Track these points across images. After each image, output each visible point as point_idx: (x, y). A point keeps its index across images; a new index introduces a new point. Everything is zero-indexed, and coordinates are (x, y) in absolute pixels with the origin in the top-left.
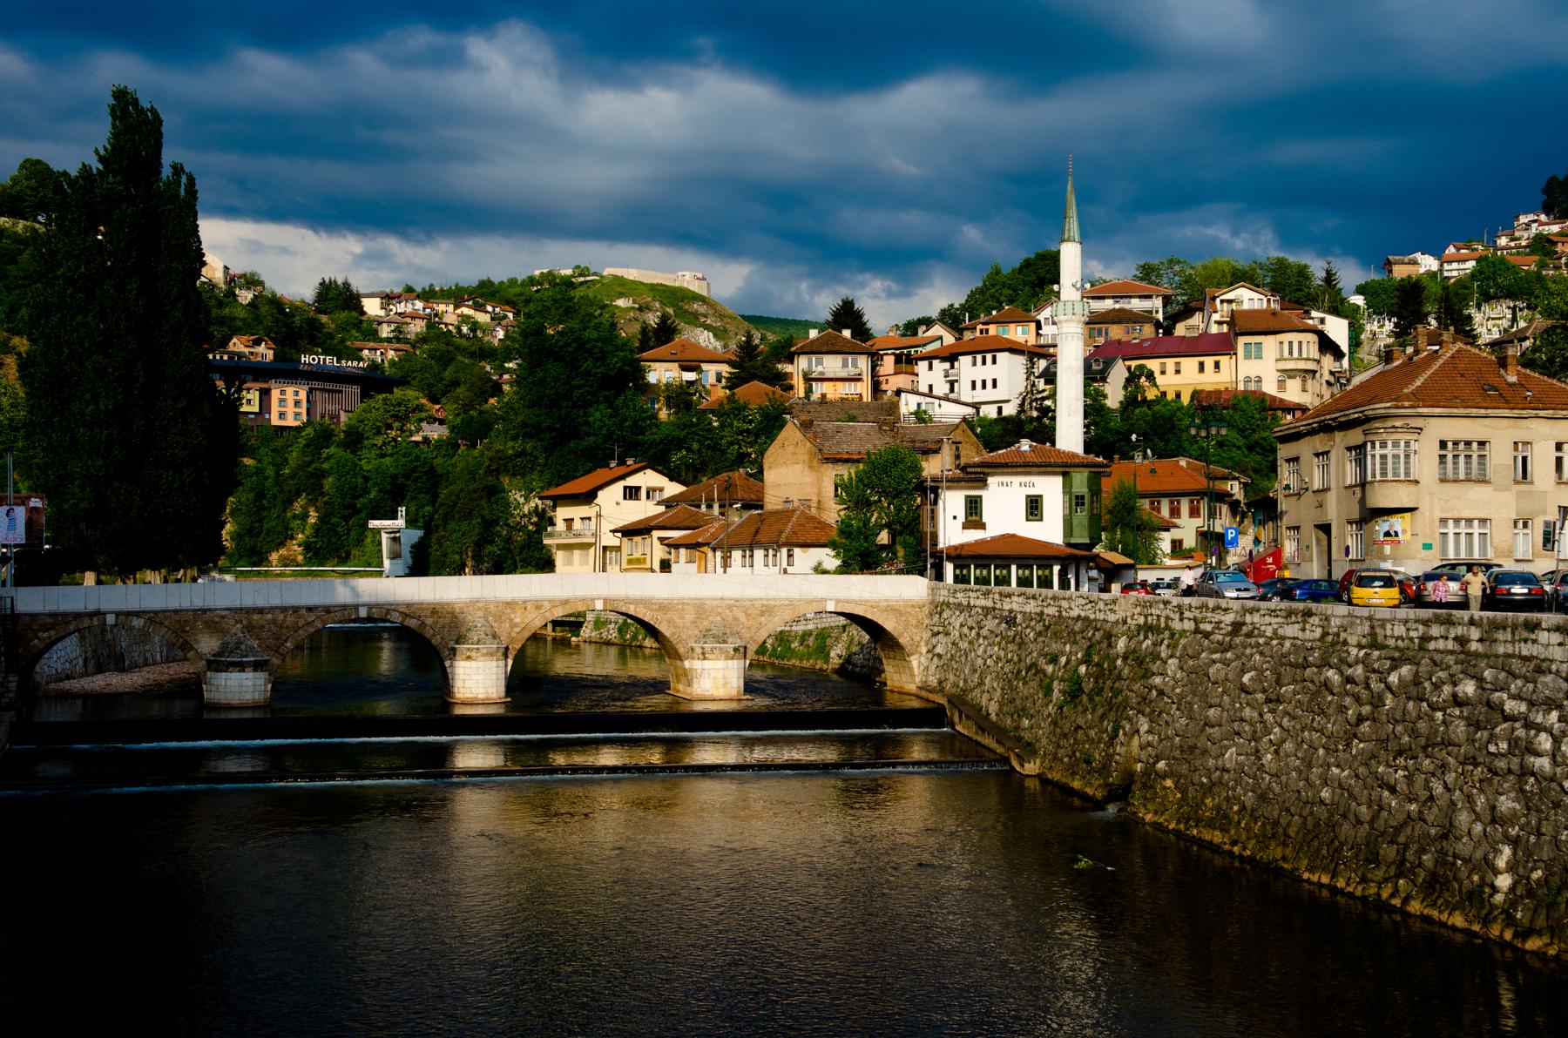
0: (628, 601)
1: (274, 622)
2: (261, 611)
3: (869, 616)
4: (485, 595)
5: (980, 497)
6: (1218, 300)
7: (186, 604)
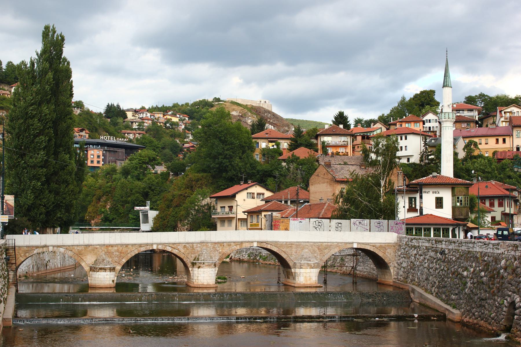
0: (267, 243)
1: (118, 251)
2: (112, 246)
3: (372, 250)
4: (206, 240)
6: (503, 112)
7: (81, 243)
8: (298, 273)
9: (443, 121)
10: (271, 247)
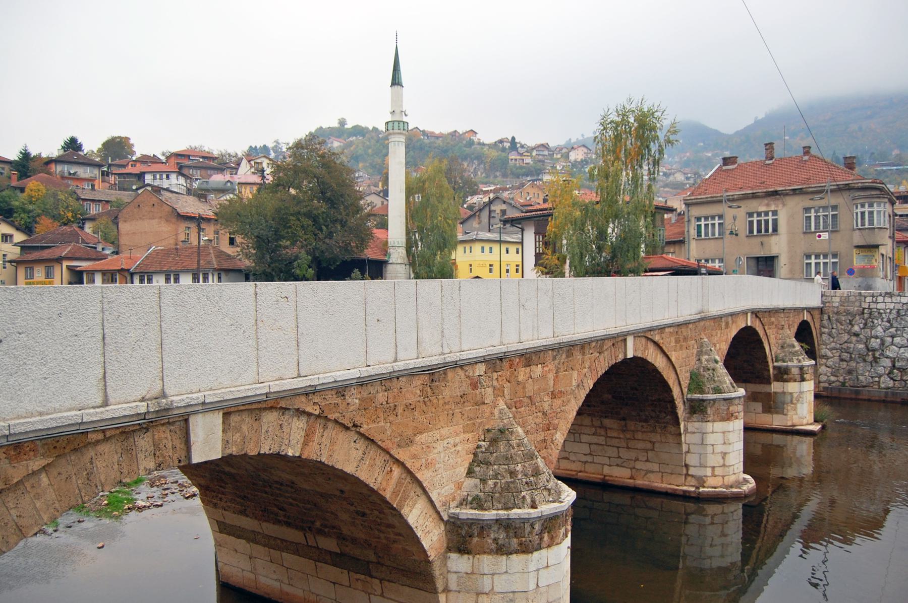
5: (777, 219)
8: (795, 395)
9: (394, 134)
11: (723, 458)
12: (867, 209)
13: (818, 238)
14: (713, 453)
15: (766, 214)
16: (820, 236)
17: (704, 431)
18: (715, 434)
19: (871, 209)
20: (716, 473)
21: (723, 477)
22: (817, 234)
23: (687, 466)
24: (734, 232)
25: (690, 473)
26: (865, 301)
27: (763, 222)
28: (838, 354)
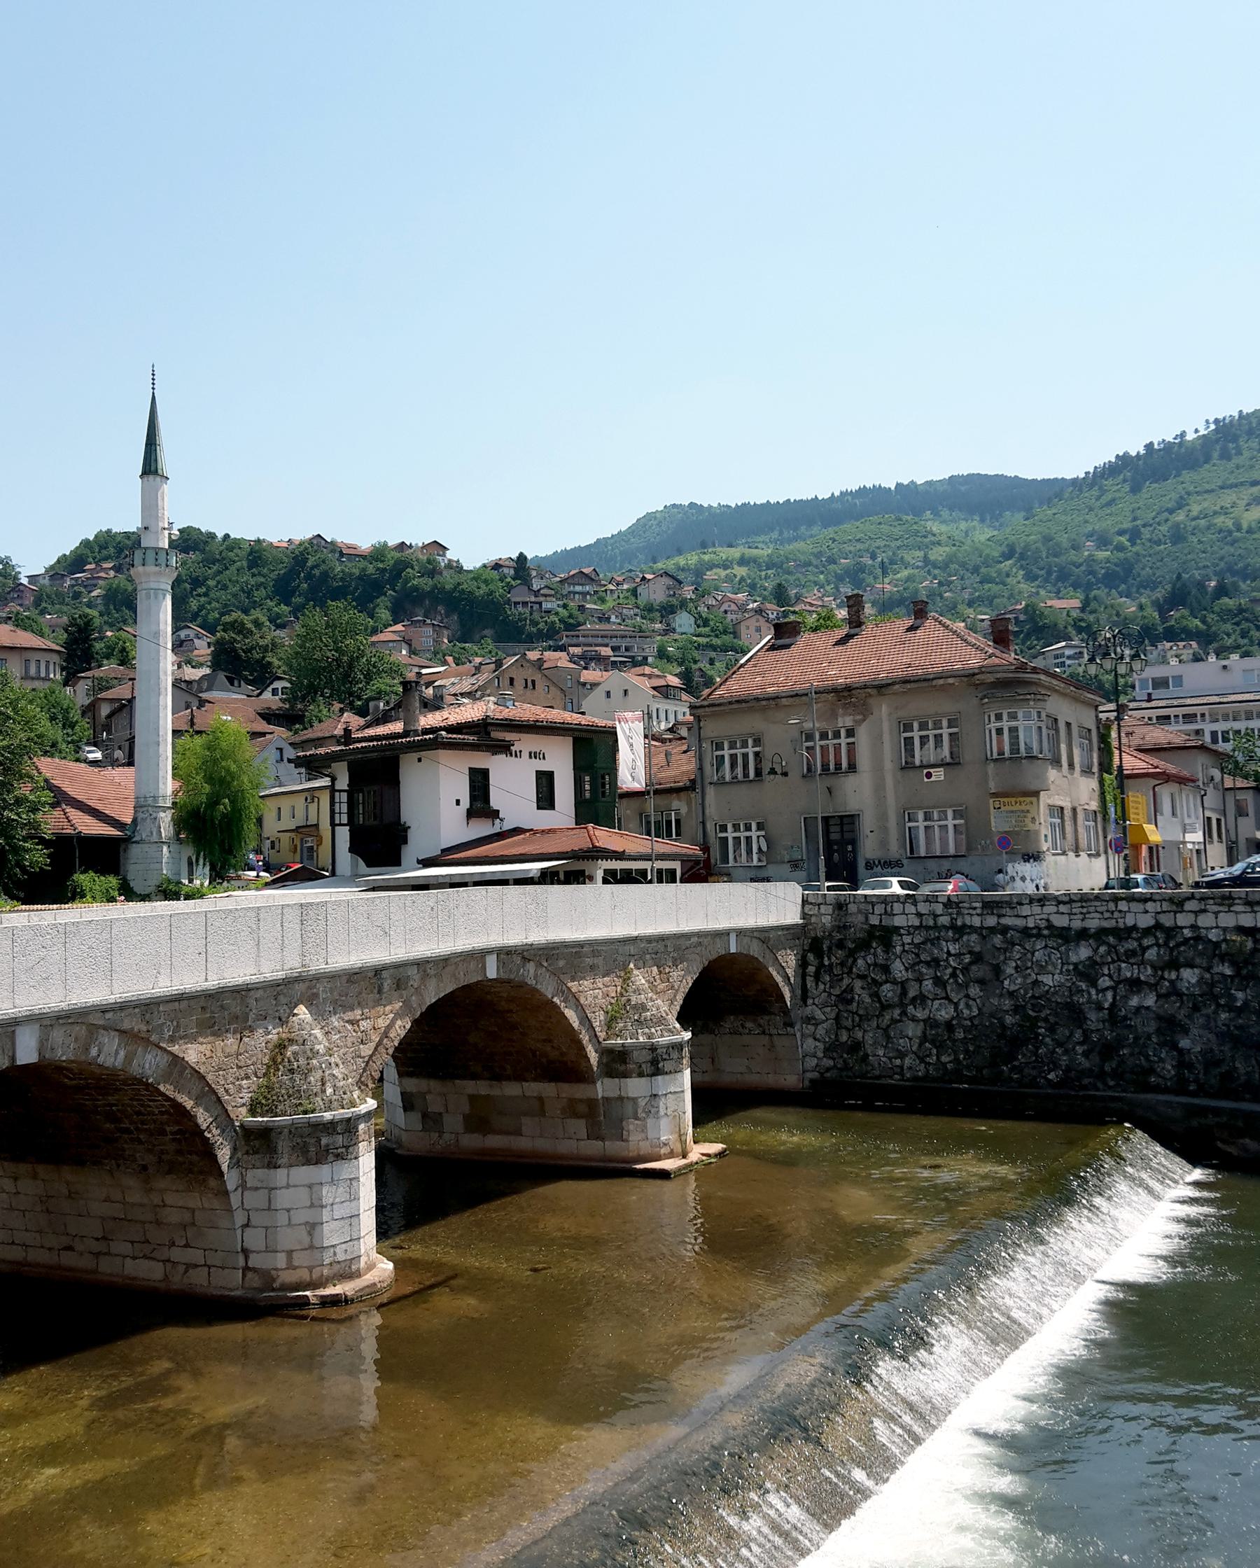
8: (642, 1103)
10: (536, 977)
11: (310, 1234)
12: (1006, 724)
13: (926, 780)
14: (289, 1224)
15: (837, 735)
16: (929, 775)
17: (272, 1186)
18: (291, 1190)
19: (1014, 724)
20: (296, 1263)
21: (311, 1269)
22: (925, 771)
23: (246, 1252)
24: (779, 770)
25: (250, 1264)
26: (873, 913)
27: (831, 750)
28: (833, 1015)
